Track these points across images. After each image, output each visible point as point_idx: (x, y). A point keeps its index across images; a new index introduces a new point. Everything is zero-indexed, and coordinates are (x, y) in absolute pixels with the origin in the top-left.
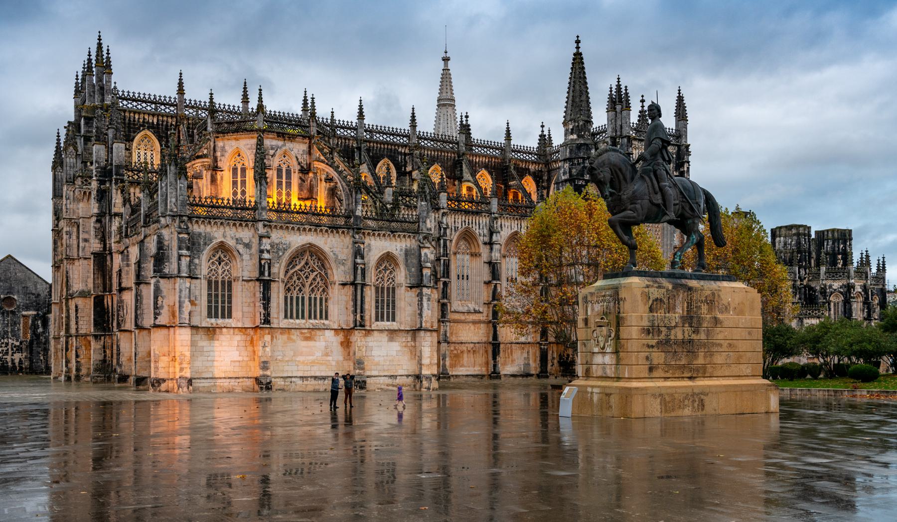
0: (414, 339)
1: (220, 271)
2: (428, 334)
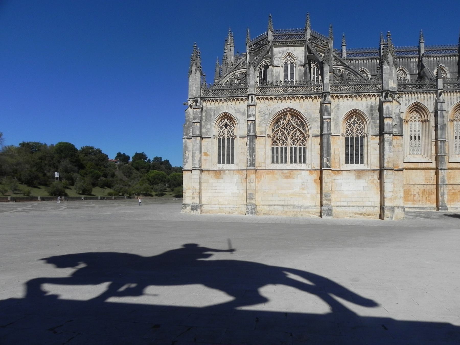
1: (226, 133)
2: (391, 172)
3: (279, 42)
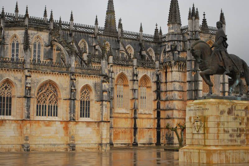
0: (98, 126)
1: (6, 93)
2: (106, 123)
3: (33, 27)
